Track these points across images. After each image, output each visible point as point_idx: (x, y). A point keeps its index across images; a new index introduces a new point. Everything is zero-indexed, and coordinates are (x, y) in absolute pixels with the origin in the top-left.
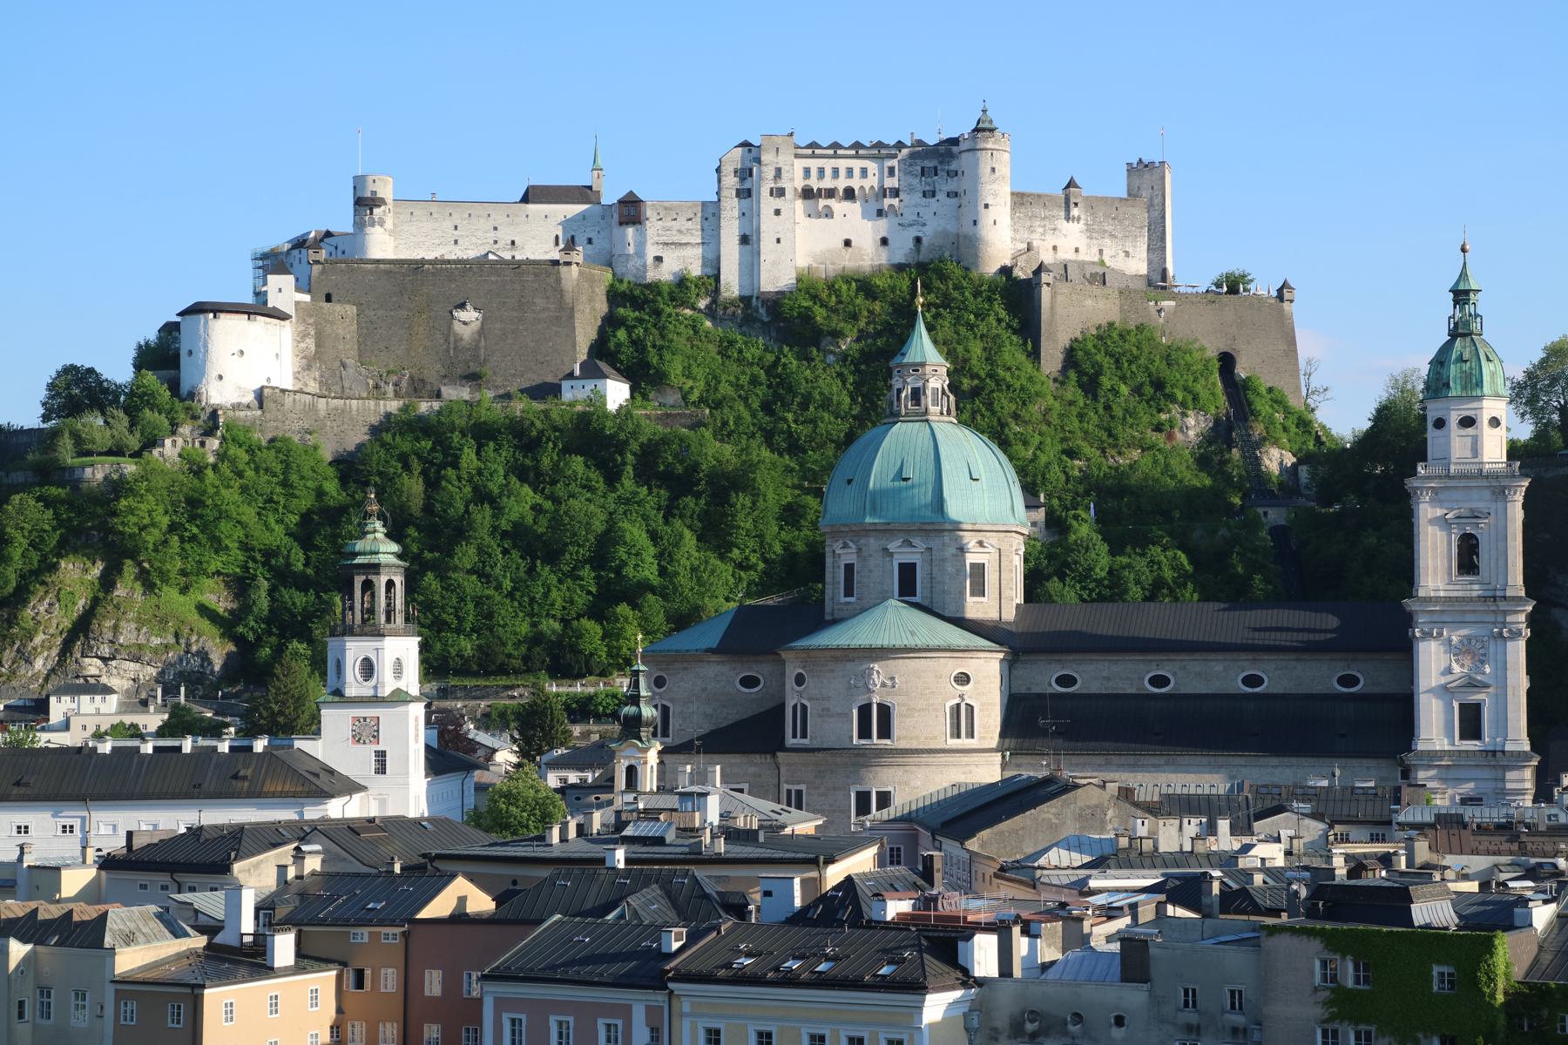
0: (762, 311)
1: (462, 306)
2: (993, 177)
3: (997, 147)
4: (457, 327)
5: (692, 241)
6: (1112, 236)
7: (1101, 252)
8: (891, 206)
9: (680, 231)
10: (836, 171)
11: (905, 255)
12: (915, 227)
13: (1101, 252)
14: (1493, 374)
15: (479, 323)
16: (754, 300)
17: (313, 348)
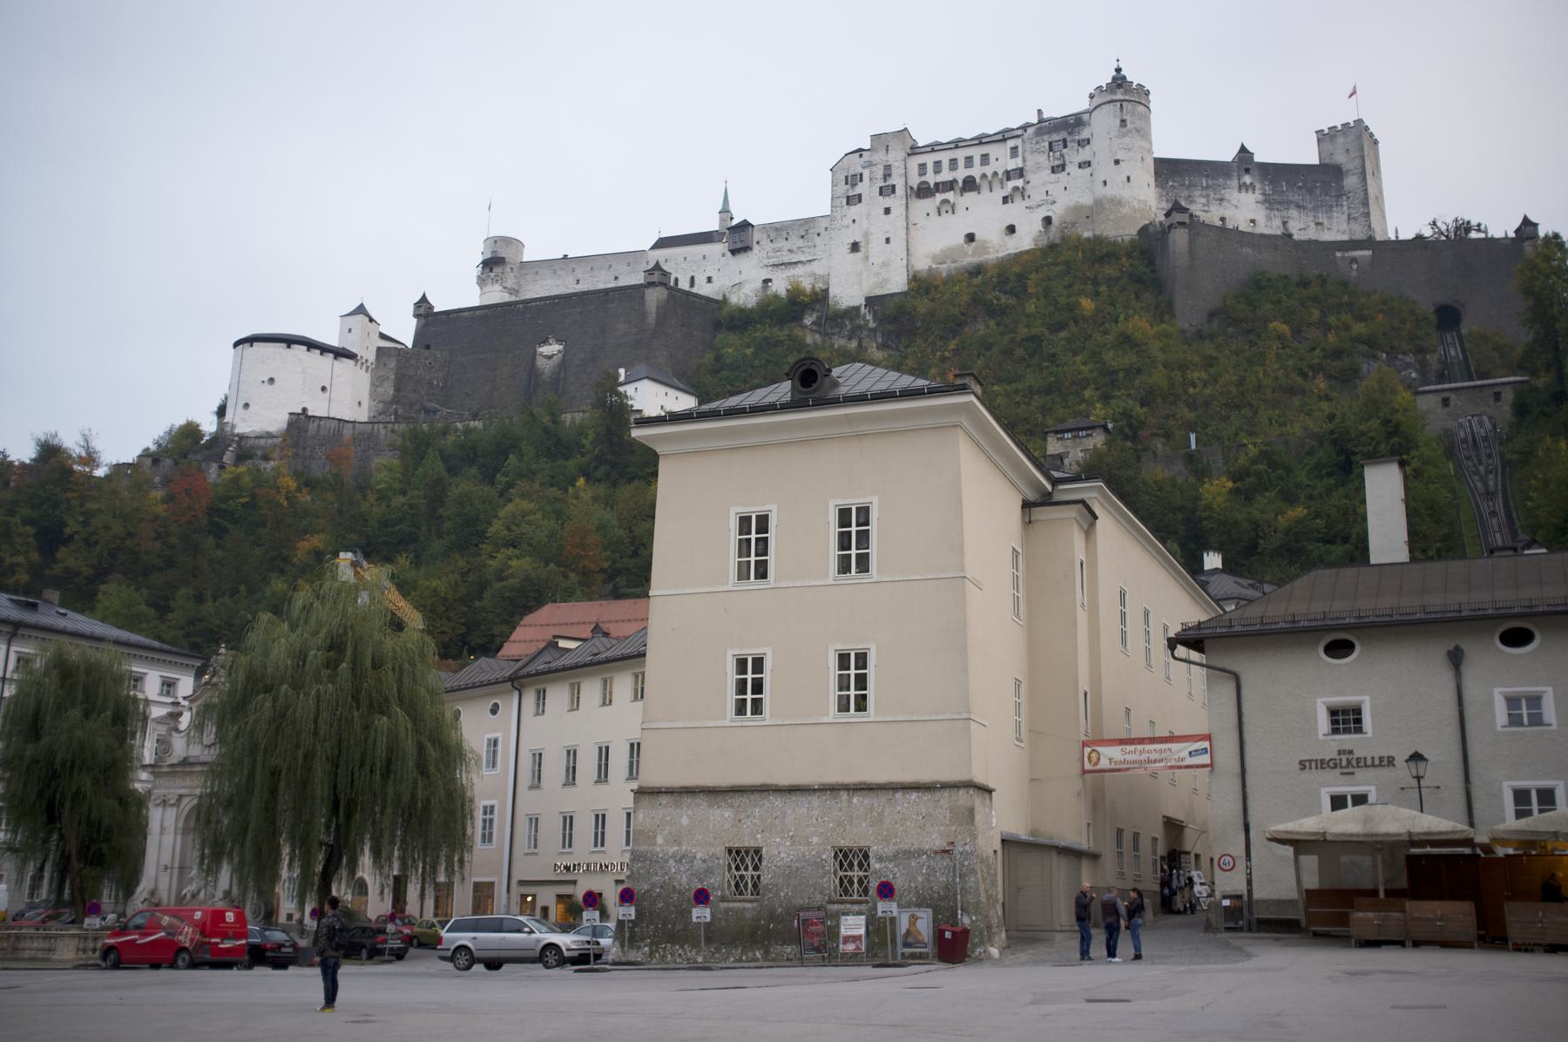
1: (545, 342)
2: (1124, 130)
3: (1127, 98)
4: (541, 363)
5: (803, 259)
6: (1299, 207)
7: (1285, 223)
8: (1016, 189)
10: (953, 162)
11: (1034, 240)
13: (1285, 223)
15: (560, 355)
16: (863, 308)
17: (391, 392)
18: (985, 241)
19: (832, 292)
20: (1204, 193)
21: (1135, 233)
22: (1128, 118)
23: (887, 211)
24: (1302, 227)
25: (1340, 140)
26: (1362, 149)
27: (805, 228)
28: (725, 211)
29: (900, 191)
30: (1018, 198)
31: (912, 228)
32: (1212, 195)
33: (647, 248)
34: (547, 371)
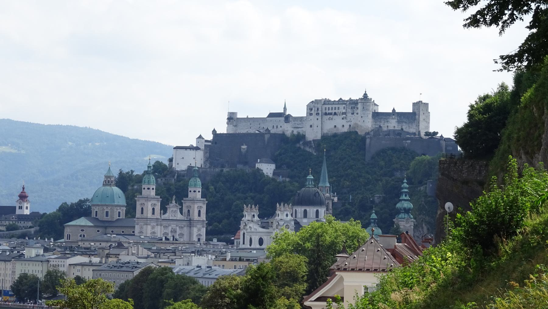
0: (313, 144)
1: (243, 145)
4: (242, 150)
6: (405, 123)
7: (402, 127)
9: (298, 124)
10: (332, 108)
12: (349, 123)
13: (402, 127)
14: (148, 181)
16: (312, 142)
17: (208, 155)
20: (384, 120)
21: (364, 133)
22: (365, 107)
23: (317, 119)
24: (406, 128)
25: (416, 106)
27: (301, 119)
28: (285, 109)
29: (320, 115)
30: (345, 119)
31: (323, 122)
32: (386, 121)
33: (266, 117)
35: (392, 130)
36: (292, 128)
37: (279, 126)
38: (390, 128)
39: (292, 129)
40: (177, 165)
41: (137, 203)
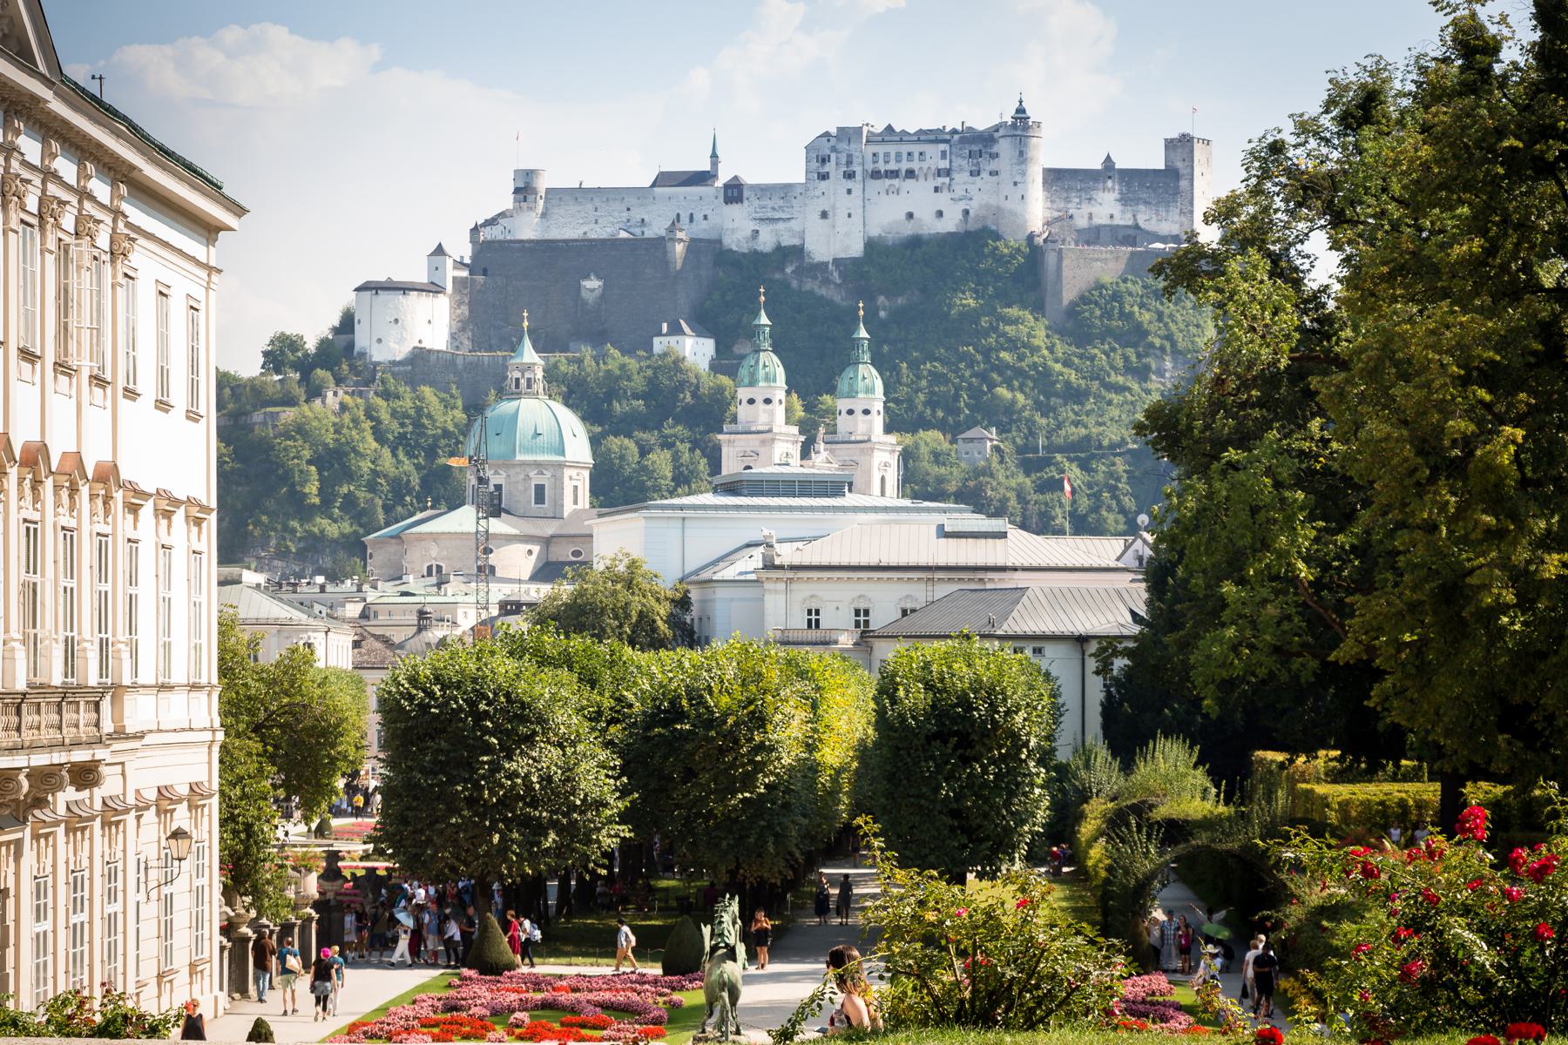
0: (836, 274)
1: (587, 277)
4: (584, 294)
6: (1146, 203)
9: (773, 209)
10: (898, 157)
17: (467, 313)
18: (920, 220)
19: (809, 246)
23: (849, 192)
24: (1147, 219)
26: (1193, 161)
27: (785, 190)
28: (714, 156)
30: (945, 191)
34: (590, 301)
35: (1105, 226)
36: (752, 223)
37: (698, 217)
38: (1097, 221)
39: (753, 226)
40: (375, 345)
41: (724, 450)
